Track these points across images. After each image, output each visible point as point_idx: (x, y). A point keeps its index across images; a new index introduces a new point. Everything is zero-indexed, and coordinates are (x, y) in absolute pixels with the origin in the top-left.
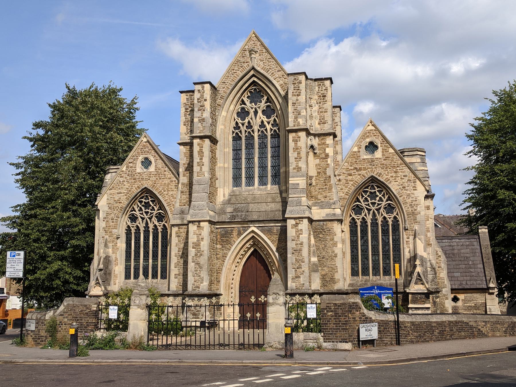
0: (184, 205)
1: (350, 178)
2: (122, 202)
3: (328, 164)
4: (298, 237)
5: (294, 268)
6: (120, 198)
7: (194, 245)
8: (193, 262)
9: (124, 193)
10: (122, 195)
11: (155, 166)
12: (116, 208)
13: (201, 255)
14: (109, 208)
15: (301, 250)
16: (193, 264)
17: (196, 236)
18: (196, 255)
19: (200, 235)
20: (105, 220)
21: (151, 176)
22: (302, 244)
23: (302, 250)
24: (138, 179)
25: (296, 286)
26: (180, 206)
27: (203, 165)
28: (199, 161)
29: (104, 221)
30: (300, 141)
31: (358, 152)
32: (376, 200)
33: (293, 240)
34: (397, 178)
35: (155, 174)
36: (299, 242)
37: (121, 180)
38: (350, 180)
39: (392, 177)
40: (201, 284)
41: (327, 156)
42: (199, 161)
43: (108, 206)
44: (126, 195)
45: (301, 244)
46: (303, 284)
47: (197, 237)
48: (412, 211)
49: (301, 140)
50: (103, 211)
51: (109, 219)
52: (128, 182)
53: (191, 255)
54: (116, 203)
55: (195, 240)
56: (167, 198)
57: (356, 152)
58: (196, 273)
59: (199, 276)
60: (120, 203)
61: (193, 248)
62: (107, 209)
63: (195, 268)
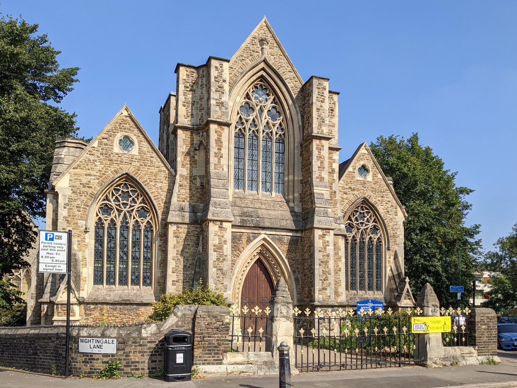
0: (184, 201)
1: (345, 196)
2: (93, 186)
3: (333, 180)
4: (325, 248)
5: (321, 280)
6: (89, 182)
7: (215, 248)
8: (214, 267)
9: (96, 176)
10: (93, 177)
11: (139, 149)
12: (84, 193)
13: (224, 260)
14: (73, 192)
15: (327, 262)
16: (214, 270)
17: (217, 238)
18: (218, 259)
19: (223, 237)
20: (67, 207)
21: (134, 160)
22: (328, 256)
23: (328, 262)
24: (115, 160)
25: (323, 298)
26: (178, 201)
27: (221, 157)
28: (216, 151)
29: (65, 208)
30: (323, 150)
31: (353, 172)
32: (363, 220)
33: (320, 251)
34: (383, 202)
35: (139, 159)
36: (325, 254)
37: (92, 158)
38: (345, 199)
39: (379, 200)
40: (225, 293)
41: (333, 171)
42: (216, 151)
43: (72, 190)
44: (98, 179)
45: (328, 256)
46: (330, 296)
47: (219, 239)
48: (393, 233)
49: (324, 149)
50: (63, 195)
51: (73, 206)
52: (102, 163)
53: (212, 259)
54: (84, 187)
55: (217, 242)
56: (154, 191)
57: (351, 172)
58: (218, 280)
59: (222, 284)
60: (88, 187)
61: (215, 251)
62: (69, 193)
63: (217, 274)
